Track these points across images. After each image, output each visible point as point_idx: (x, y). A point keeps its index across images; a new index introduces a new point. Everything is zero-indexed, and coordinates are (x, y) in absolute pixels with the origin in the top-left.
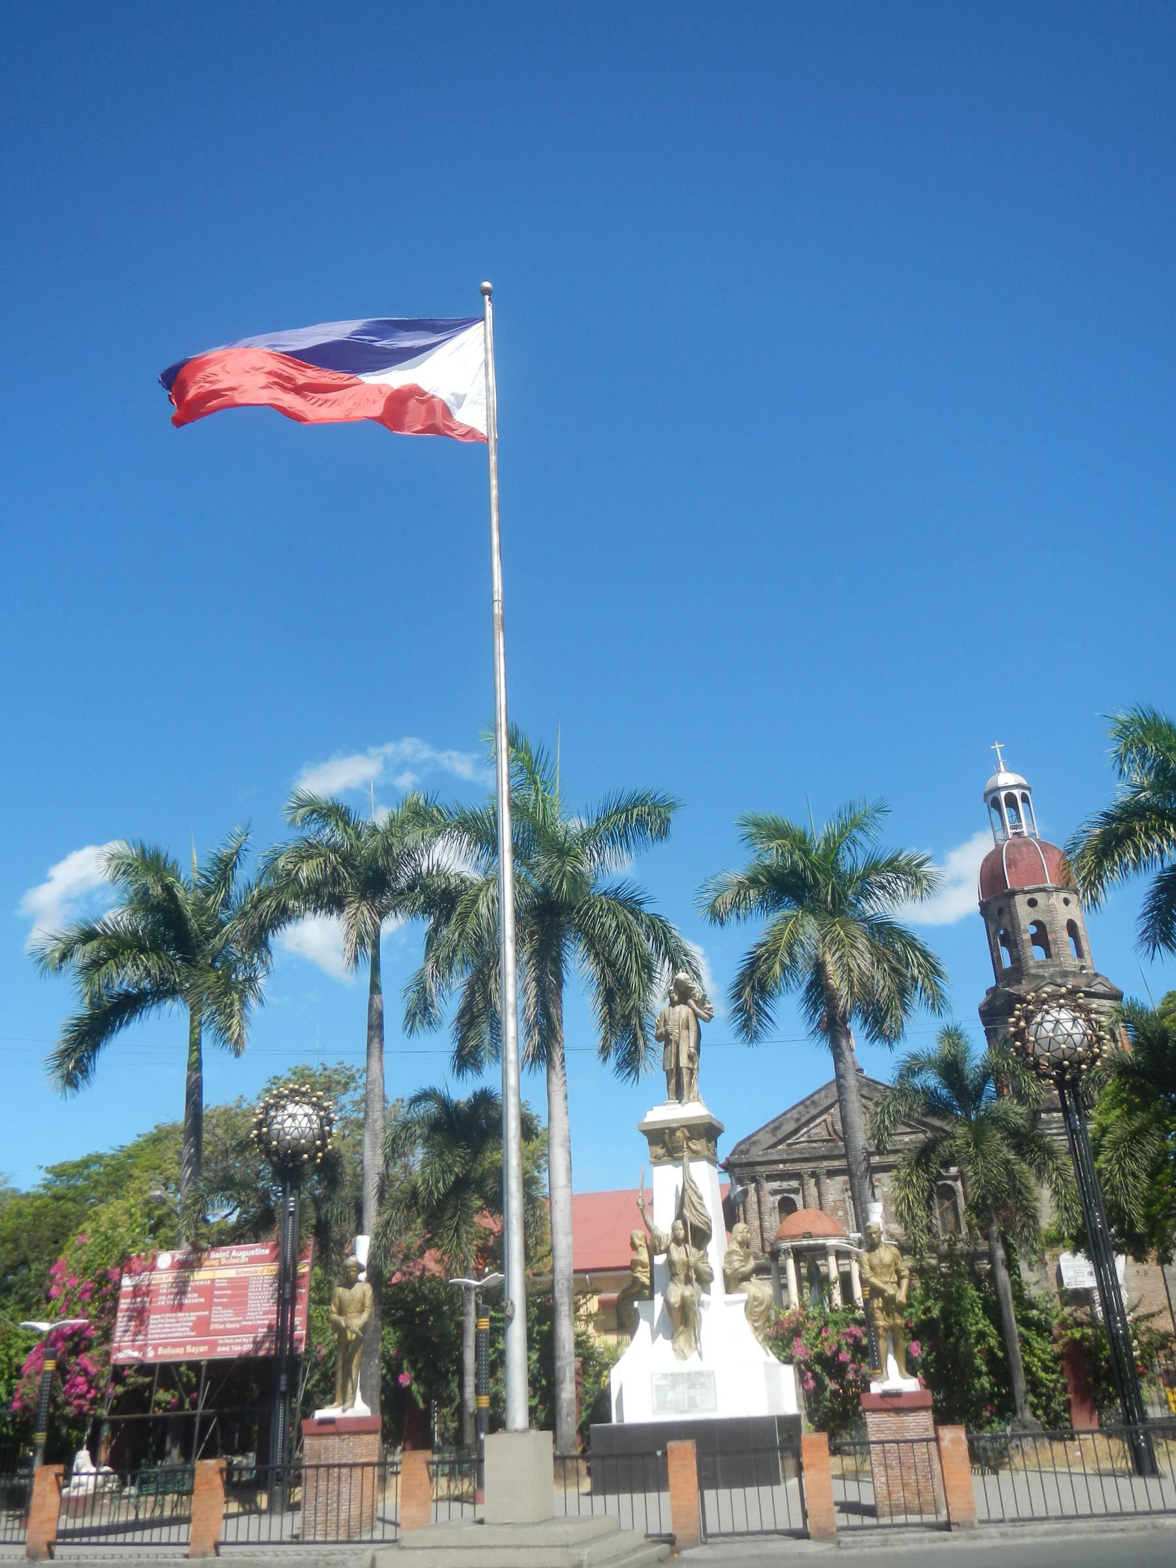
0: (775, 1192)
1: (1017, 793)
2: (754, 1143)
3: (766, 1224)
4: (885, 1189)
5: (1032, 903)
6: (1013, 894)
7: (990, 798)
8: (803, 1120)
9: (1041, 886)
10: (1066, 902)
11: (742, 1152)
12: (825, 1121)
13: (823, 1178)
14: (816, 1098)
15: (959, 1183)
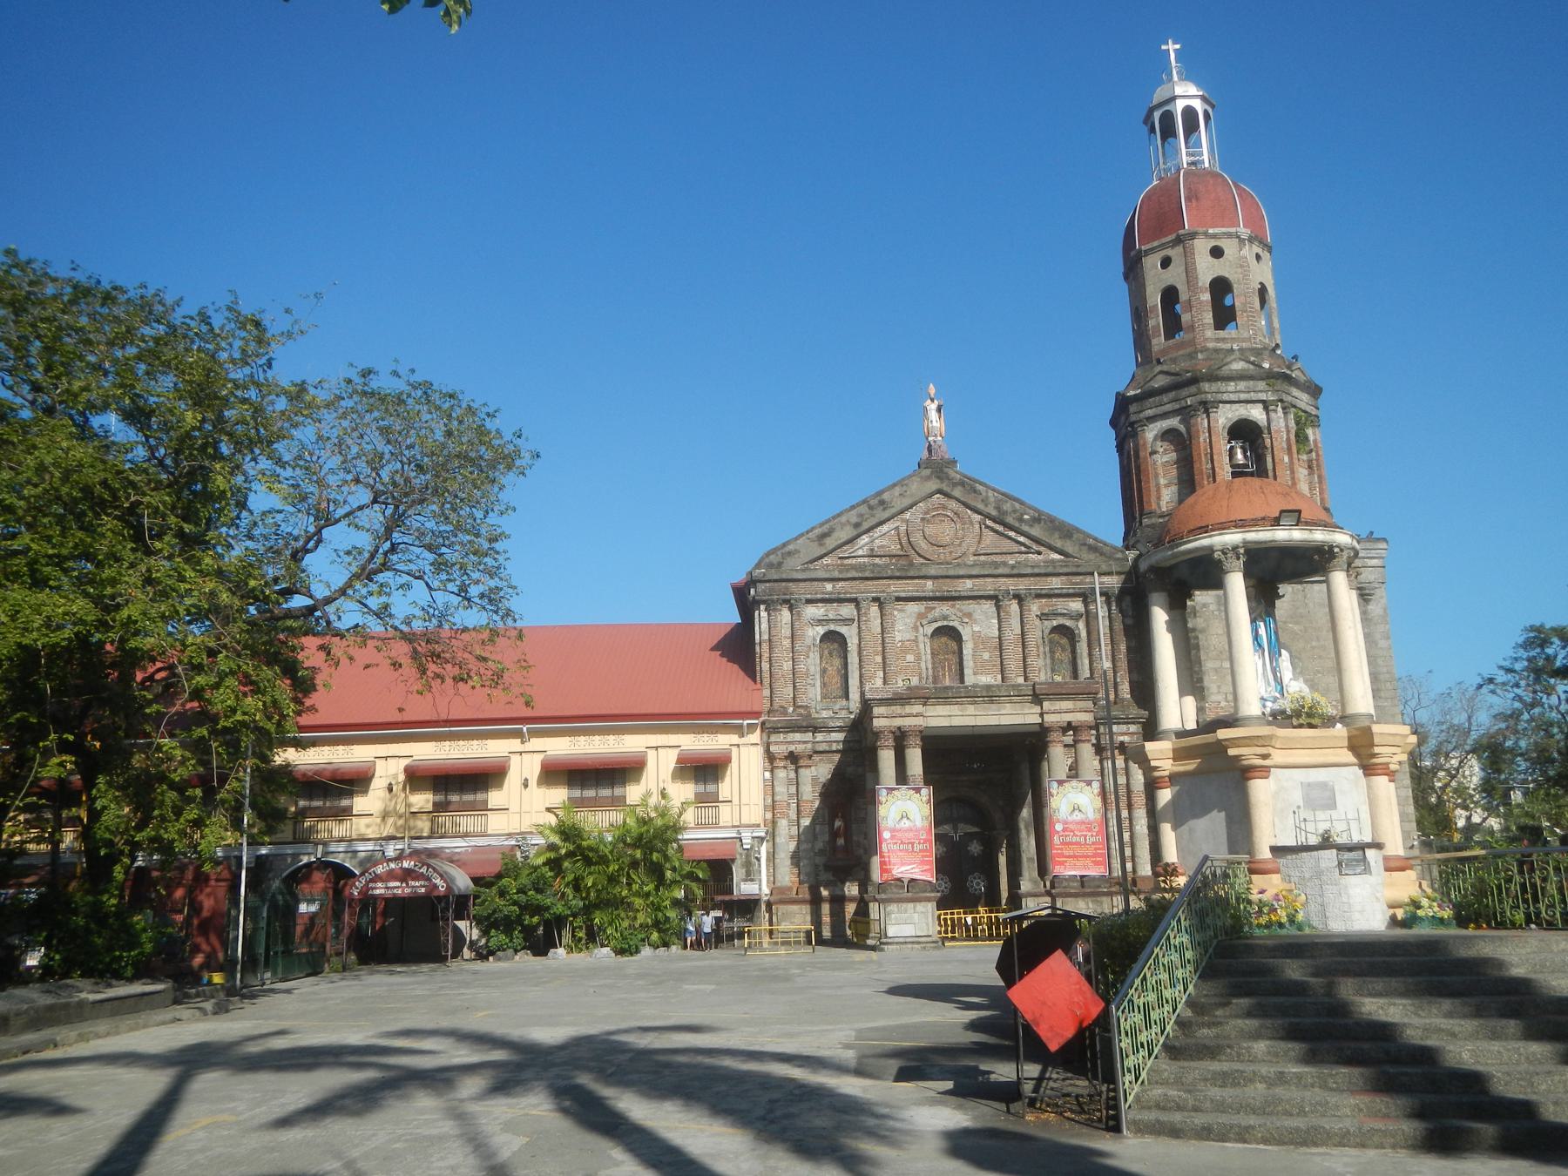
0: (820, 622)
1: (1198, 105)
2: (789, 553)
3: (801, 667)
4: (977, 629)
5: (1217, 252)
6: (1193, 236)
7: (1157, 115)
8: (866, 526)
9: (1233, 230)
10: (1258, 257)
11: (771, 566)
12: (897, 528)
13: (888, 608)
14: (886, 496)
15: (1081, 625)
